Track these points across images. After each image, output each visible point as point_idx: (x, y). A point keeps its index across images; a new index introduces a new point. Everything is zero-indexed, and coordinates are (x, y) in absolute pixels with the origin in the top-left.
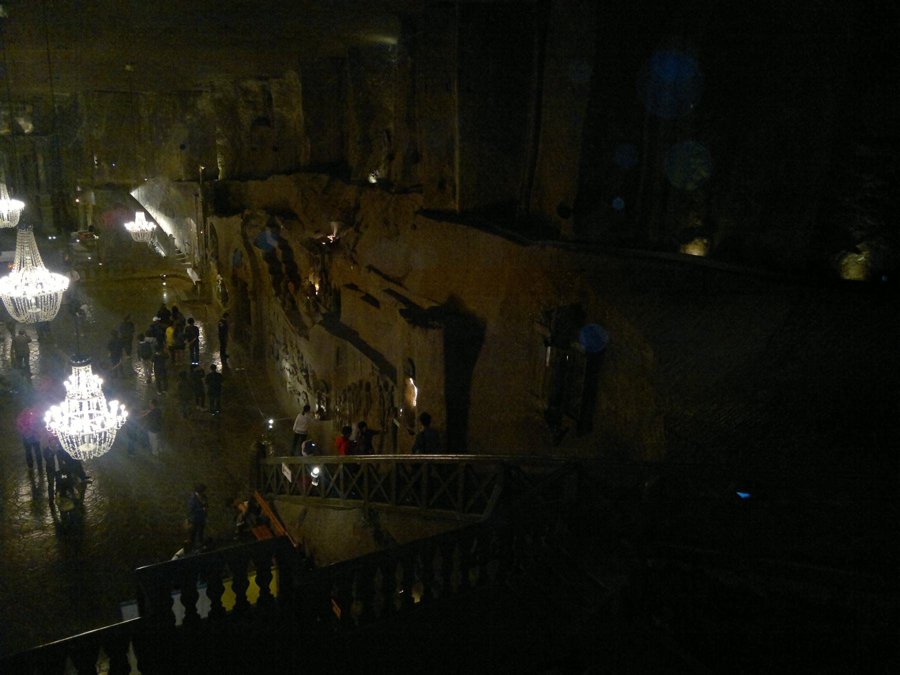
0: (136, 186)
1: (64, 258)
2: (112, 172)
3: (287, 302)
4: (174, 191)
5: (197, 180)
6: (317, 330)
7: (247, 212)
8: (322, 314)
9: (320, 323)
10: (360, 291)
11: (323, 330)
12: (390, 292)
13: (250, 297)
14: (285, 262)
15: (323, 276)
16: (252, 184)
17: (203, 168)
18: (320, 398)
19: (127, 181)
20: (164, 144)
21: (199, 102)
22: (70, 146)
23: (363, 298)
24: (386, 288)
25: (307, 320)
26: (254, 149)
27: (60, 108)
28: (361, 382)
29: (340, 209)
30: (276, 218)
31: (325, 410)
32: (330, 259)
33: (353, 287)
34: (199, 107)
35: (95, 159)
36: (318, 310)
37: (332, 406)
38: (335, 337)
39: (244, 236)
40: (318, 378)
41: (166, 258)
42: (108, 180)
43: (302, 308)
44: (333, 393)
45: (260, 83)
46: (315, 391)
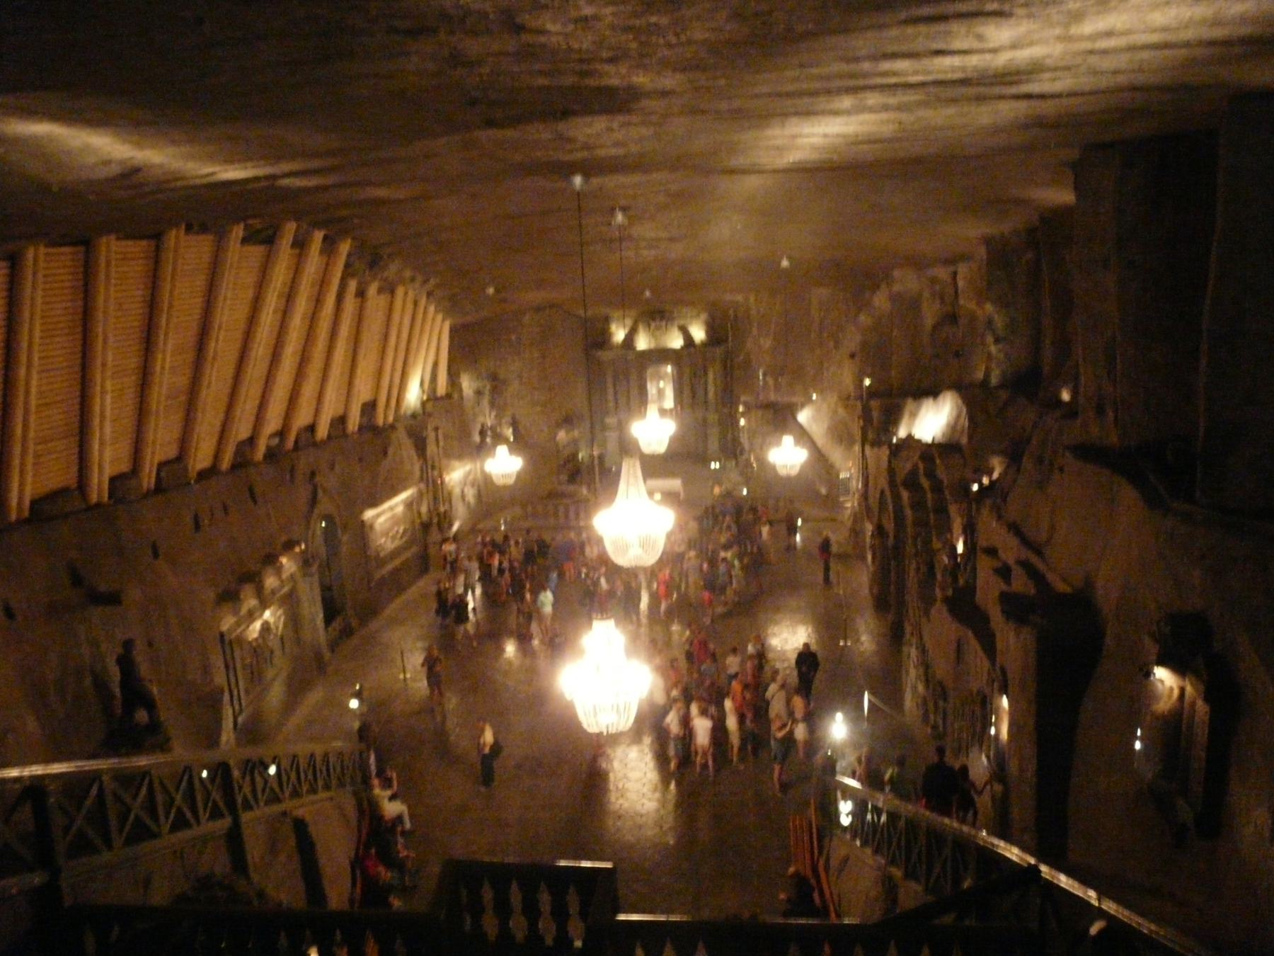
0: (803, 406)
1: (712, 491)
2: (777, 388)
3: (921, 567)
4: (841, 411)
5: (861, 398)
6: (940, 612)
9: (946, 600)
10: (998, 558)
11: (945, 609)
12: (1025, 564)
15: (968, 532)
17: (867, 382)
18: (936, 704)
19: (794, 399)
22: (742, 358)
23: (997, 571)
24: (1023, 557)
25: (938, 591)
31: (941, 729)
32: (978, 510)
36: (955, 579)
37: (950, 718)
39: (891, 472)
41: (827, 496)
42: (772, 397)
43: (939, 577)
45: (951, 269)
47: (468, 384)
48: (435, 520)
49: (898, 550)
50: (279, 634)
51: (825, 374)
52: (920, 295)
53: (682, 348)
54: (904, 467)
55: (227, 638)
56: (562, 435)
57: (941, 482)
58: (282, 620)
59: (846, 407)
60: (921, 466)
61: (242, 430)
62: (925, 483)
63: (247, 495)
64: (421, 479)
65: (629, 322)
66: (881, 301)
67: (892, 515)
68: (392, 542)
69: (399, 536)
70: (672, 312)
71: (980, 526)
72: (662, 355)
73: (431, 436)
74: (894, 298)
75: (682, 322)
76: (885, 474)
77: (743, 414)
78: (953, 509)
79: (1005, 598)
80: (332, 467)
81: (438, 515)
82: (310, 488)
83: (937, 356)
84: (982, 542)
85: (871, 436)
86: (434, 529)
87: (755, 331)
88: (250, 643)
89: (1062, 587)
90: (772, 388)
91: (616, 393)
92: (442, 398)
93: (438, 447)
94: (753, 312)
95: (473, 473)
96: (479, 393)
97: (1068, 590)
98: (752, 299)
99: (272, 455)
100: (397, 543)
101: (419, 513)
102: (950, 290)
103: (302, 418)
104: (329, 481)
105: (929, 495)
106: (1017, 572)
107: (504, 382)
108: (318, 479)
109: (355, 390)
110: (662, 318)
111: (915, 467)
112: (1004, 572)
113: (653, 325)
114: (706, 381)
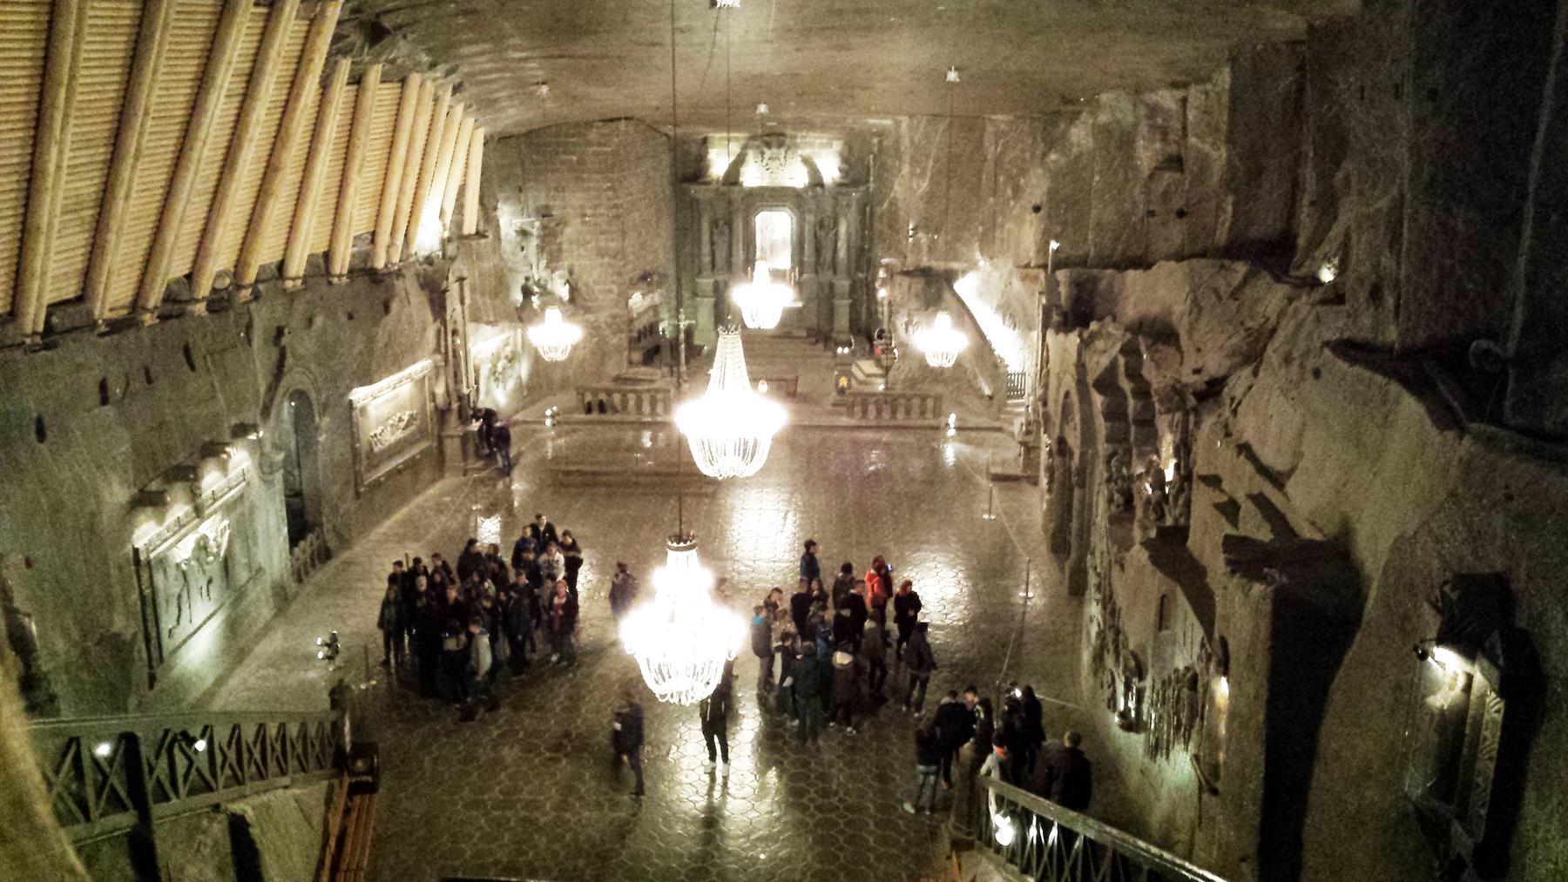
5: (1044, 266)
6: (1139, 554)
7: (1094, 326)
8: (1163, 532)
9: (1147, 544)
10: (1222, 491)
12: (1260, 501)
13: (1074, 479)
14: (1138, 423)
16: (1132, 274)
17: (1054, 245)
18: (1128, 687)
19: (955, 265)
20: (1012, 203)
21: (1074, 130)
22: (886, 205)
23: (1217, 506)
24: (1256, 491)
25: (1137, 534)
26: (1151, 214)
27: (880, 142)
28: (1187, 669)
29: (1247, 330)
30: (1141, 339)
31: (1133, 714)
32: (1197, 424)
33: (1213, 481)
34: (1074, 139)
35: (911, 226)
36: (1161, 517)
37: (1145, 707)
38: (1159, 574)
39: (1081, 366)
40: (1131, 646)
41: (991, 398)
42: (925, 261)
43: (1139, 513)
44: (1148, 683)
45: (1179, 94)
46: (1124, 672)
47: (509, 219)
48: (455, 406)
49: (1084, 473)
50: (222, 553)
51: (998, 234)
52: (1135, 125)
53: (806, 189)
54: (1098, 363)
55: (143, 557)
56: (637, 301)
57: (1148, 384)
58: (228, 532)
59: (1024, 279)
60: (1122, 361)
61: (175, 265)
62: (1126, 385)
63: (181, 356)
64: (437, 350)
65: (735, 148)
66: (1080, 135)
67: (1078, 427)
68: (393, 434)
69: (402, 425)
70: (794, 137)
71: (1199, 448)
72: (774, 196)
73: (454, 288)
74: (1103, 133)
75: (807, 152)
76: (1072, 369)
77: (884, 283)
78: (1162, 422)
79: (1230, 544)
80: (310, 321)
81: (460, 398)
82: (274, 353)
83: (1151, 214)
84: (1201, 468)
85: (1056, 318)
86: (453, 418)
87: (906, 169)
88: (178, 566)
89: (1308, 533)
90: (925, 249)
91: (712, 244)
92: (468, 237)
93: (462, 302)
94: (906, 142)
95: (511, 340)
96: (524, 233)
97: (1318, 537)
98: (904, 126)
99: (219, 303)
100: (400, 434)
101: (433, 396)
102: (1176, 125)
103: (265, 253)
104: (302, 344)
105: (1131, 402)
106: (1247, 507)
107: (563, 222)
108: (285, 341)
109: (345, 219)
110: (781, 145)
111: (1113, 365)
112: (1230, 510)
113: (768, 153)
114: (836, 235)
